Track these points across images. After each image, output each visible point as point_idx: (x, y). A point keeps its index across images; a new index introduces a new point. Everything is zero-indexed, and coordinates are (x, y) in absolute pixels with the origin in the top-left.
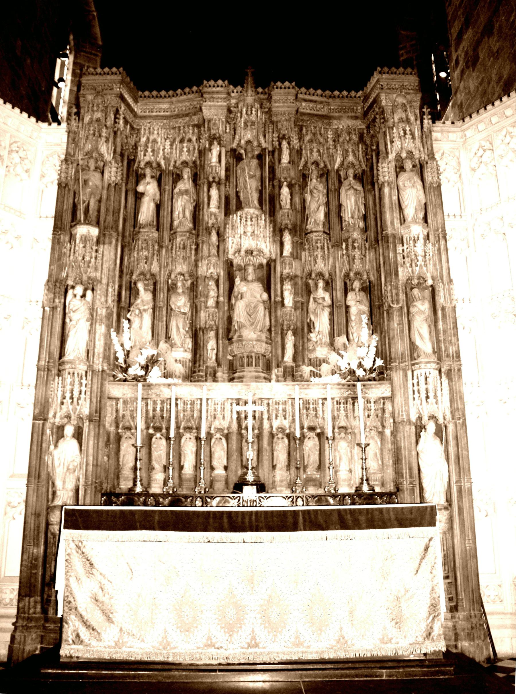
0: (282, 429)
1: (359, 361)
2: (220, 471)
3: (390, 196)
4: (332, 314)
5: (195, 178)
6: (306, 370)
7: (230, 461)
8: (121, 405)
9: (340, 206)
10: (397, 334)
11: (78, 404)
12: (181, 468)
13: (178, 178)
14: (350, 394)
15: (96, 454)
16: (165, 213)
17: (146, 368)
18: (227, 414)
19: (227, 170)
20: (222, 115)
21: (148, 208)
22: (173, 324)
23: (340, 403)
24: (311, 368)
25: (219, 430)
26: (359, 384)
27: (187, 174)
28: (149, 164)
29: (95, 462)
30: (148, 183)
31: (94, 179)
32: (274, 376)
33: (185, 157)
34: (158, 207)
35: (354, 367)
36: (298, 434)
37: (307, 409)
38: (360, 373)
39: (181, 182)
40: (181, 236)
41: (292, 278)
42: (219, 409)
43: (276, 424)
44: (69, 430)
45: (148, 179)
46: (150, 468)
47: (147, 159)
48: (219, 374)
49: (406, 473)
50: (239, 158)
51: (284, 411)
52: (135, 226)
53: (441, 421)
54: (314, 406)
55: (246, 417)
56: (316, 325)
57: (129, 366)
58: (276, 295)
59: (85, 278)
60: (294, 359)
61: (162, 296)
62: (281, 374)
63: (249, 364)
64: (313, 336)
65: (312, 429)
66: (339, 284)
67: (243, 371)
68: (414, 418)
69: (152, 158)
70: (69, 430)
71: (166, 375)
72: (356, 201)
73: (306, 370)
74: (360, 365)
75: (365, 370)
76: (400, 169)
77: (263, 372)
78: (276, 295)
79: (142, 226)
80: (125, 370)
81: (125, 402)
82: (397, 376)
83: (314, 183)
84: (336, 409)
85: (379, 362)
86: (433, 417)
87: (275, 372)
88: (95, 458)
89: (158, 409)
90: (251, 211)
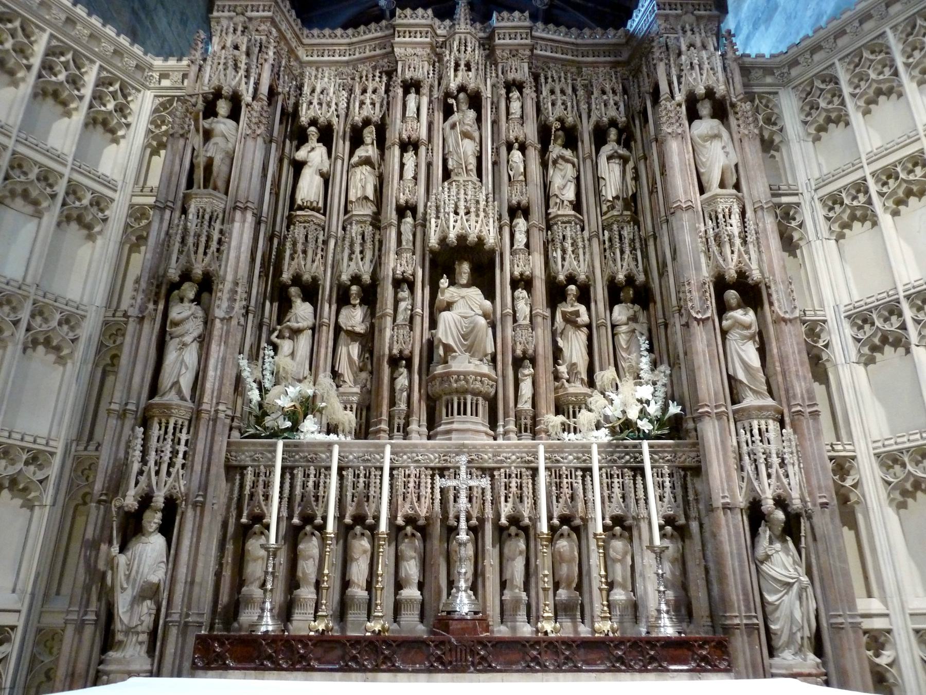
0: (514, 520)
1: (640, 407)
2: (411, 592)
3: (681, 153)
7: (427, 574)
8: (249, 477)
9: (597, 179)
10: (705, 361)
11: (169, 474)
12: (346, 584)
13: (356, 140)
14: (627, 462)
15: (191, 562)
16: (336, 190)
17: (295, 417)
18: (425, 491)
19: (430, 125)
20: (424, 52)
21: (311, 182)
22: (343, 350)
23: (612, 476)
24: (561, 418)
25: (410, 520)
26: (645, 444)
27: (369, 135)
28: (314, 122)
29: (189, 575)
30: (313, 149)
32: (500, 430)
33: (367, 111)
35: (633, 414)
36: (544, 527)
37: (559, 486)
38: (645, 426)
39: (362, 147)
40: (358, 222)
42: (411, 485)
43: (506, 510)
44: (153, 519)
45: (313, 141)
47: (311, 114)
48: (414, 426)
49: (738, 600)
50: (448, 112)
51: (520, 487)
52: (291, 208)
53: (796, 504)
54: (569, 480)
55: (456, 498)
56: (566, 352)
57: (265, 414)
58: (503, 306)
59: (198, 271)
60: (534, 405)
61: (328, 310)
62: (512, 426)
63: (462, 411)
64: (563, 369)
65: (565, 520)
66: (600, 293)
67: (452, 423)
68: (741, 500)
69: (319, 112)
70: (153, 519)
72: (624, 172)
73: (553, 420)
74: (643, 414)
75: (651, 421)
77: (483, 425)
78: (503, 306)
79: (301, 208)
80: (260, 420)
81: (256, 475)
82: (710, 431)
84: (605, 485)
86: (781, 502)
88: (191, 568)
89: (311, 484)
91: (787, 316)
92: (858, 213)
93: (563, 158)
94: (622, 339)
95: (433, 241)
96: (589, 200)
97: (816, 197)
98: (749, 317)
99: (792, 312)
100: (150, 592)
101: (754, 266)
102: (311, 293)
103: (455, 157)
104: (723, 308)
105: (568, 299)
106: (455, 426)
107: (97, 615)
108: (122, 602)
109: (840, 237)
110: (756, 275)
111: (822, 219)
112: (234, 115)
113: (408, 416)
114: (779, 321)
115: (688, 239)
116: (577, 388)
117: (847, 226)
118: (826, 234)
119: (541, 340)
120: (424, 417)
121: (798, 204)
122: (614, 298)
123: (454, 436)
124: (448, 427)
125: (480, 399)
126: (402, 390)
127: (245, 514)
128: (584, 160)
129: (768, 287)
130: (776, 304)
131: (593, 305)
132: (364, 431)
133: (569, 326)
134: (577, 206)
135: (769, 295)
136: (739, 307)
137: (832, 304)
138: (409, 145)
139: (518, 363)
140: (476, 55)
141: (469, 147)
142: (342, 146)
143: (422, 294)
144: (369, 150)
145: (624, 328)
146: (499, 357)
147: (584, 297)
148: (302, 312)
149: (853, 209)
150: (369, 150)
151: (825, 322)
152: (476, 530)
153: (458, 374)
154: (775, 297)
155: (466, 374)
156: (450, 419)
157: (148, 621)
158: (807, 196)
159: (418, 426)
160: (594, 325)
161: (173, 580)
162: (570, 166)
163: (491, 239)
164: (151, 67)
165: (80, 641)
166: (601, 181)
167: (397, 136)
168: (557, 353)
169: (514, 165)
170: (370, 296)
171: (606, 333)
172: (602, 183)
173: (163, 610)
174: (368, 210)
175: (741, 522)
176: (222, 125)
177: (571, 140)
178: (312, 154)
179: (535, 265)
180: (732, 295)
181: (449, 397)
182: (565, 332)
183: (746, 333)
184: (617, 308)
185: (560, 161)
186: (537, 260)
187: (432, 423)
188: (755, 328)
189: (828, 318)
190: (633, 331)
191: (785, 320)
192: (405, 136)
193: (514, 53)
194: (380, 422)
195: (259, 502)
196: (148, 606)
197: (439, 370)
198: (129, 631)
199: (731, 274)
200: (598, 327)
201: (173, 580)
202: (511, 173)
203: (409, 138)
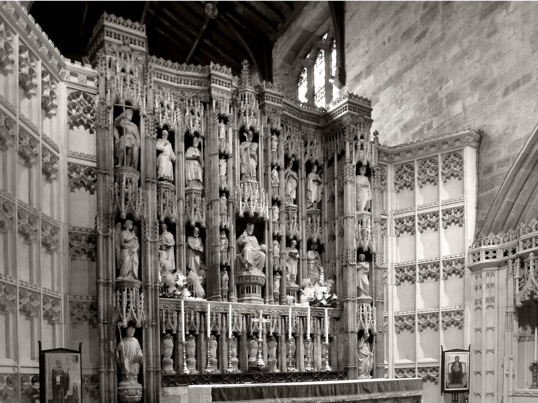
4: (299, 264)
89: (192, 318)
91: (380, 267)
92: (408, 229)
93: (293, 176)
94: (312, 266)
97: (393, 218)
98: (366, 265)
99: (381, 265)
100: (138, 360)
101: (374, 246)
103: (246, 167)
104: (359, 260)
105: (292, 246)
106: (252, 298)
107: (114, 369)
108: (126, 363)
109: (399, 236)
110: (374, 250)
111: (394, 228)
113: (229, 292)
114: (377, 268)
115: (350, 231)
117: (402, 232)
118: (394, 235)
120: (236, 293)
121: (386, 219)
123: (252, 301)
124: (249, 298)
125: (257, 286)
126: (226, 281)
127: (164, 329)
128: (302, 179)
129: (375, 255)
130: (377, 262)
131: (301, 250)
133: (291, 258)
135: (375, 258)
136: (364, 261)
137: (391, 262)
139: (275, 273)
141: (253, 163)
145: (313, 262)
146: (267, 270)
149: (407, 226)
151: (387, 268)
153: (254, 276)
154: (377, 259)
155: (257, 277)
156: (249, 294)
157: (137, 371)
158: (390, 217)
159: (234, 296)
160: (301, 259)
161: (147, 355)
162: (295, 181)
164: (65, 66)
165: (109, 379)
166: (309, 192)
167: (218, 149)
169: (274, 178)
171: (306, 262)
172: (309, 193)
173: (144, 367)
178: (165, 147)
180: (363, 256)
181: (248, 285)
182: (289, 260)
183: (366, 271)
184: (309, 252)
185: (291, 177)
186: (283, 227)
188: (368, 270)
189: (388, 267)
190: (316, 263)
191: (379, 268)
192: (222, 151)
194: (218, 294)
195: (169, 324)
196: (137, 366)
197: (245, 273)
198: (131, 374)
199: (365, 249)
200: (303, 260)
201: (147, 355)
202: (273, 182)
203: (224, 152)
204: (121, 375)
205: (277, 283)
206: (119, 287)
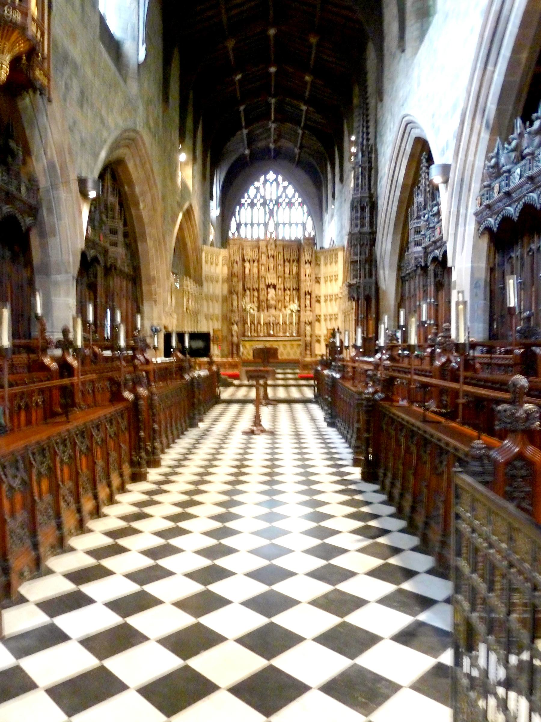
5: (258, 261)
6: (283, 309)
13: (254, 261)
31: (235, 265)
34: (250, 270)
41: (280, 289)
46: (251, 329)
61: (252, 293)
66: (292, 289)
71: (253, 310)
73: (283, 309)
76: (306, 263)
83: (287, 264)
85: (299, 309)
87: (277, 310)
90: (272, 271)
95: (267, 283)
96: (291, 273)
102: (250, 290)
104: (306, 295)
112: (237, 263)
116: (287, 304)
119: (282, 298)
122: (293, 289)
132: (258, 311)
134: (289, 274)
138: (263, 265)
140: (273, 247)
141: (272, 266)
142: (252, 262)
143: (265, 289)
144: (256, 264)
147: (289, 290)
148: (248, 292)
150: (256, 264)
152: (273, 325)
159: (266, 310)
163: (275, 283)
168: (285, 298)
170: (258, 290)
174: (256, 276)
175: (304, 324)
176: (235, 265)
177: (289, 261)
179: (282, 287)
187: (267, 309)
193: (280, 245)
204: (232, 335)
205: (280, 305)
206: (232, 311)
